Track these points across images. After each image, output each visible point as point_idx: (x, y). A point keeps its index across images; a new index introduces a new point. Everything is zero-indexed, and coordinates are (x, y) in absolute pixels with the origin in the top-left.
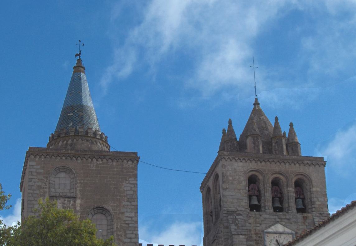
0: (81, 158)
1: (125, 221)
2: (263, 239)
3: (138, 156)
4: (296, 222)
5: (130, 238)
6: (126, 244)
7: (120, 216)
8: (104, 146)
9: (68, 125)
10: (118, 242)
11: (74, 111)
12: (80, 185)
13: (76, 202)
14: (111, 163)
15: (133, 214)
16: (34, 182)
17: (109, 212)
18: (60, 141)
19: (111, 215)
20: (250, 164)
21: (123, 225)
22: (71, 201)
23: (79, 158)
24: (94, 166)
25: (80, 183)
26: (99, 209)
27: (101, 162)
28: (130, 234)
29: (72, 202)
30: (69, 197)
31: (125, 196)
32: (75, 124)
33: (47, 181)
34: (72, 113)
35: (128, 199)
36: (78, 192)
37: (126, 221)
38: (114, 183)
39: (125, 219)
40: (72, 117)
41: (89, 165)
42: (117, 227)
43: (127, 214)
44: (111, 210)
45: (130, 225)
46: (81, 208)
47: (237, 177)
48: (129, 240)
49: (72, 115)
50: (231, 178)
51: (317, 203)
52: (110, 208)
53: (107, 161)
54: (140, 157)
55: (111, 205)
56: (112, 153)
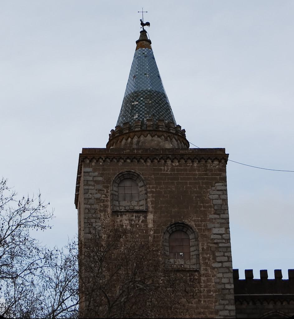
0: (150, 159)
1: (212, 239)
3: (226, 153)
6: (216, 270)
8: (181, 143)
9: (132, 118)
10: (205, 268)
11: (140, 99)
12: (151, 195)
13: (148, 217)
14: (191, 164)
15: (222, 231)
16: (91, 194)
17: (191, 228)
18: (122, 140)
19: (194, 232)
21: (211, 245)
22: (140, 216)
23: (149, 160)
24: (168, 169)
25: (152, 192)
26: (178, 226)
27: (178, 164)
28: (221, 256)
29: (142, 218)
30: (137, 212)
31: (211, 207)
32: (141, 116)
33: (107, 192)
34: (137, 101)
35: (216, 210)
36: (150, 205)
37: (215, 239)
38: (195, 190)
39: (212, 237)
40: (137, 106)
41: (163, 168)
42: (203, 249)
43: (215, 231)
44: (194, 226)
45: (220, 245)
46: (154, 225)
48: (220, 265)
49: (137, 104)
52: (192, 224)
53: (186, 162)
54: (228, 154)
55: (194, 219)
56: (191, 151)
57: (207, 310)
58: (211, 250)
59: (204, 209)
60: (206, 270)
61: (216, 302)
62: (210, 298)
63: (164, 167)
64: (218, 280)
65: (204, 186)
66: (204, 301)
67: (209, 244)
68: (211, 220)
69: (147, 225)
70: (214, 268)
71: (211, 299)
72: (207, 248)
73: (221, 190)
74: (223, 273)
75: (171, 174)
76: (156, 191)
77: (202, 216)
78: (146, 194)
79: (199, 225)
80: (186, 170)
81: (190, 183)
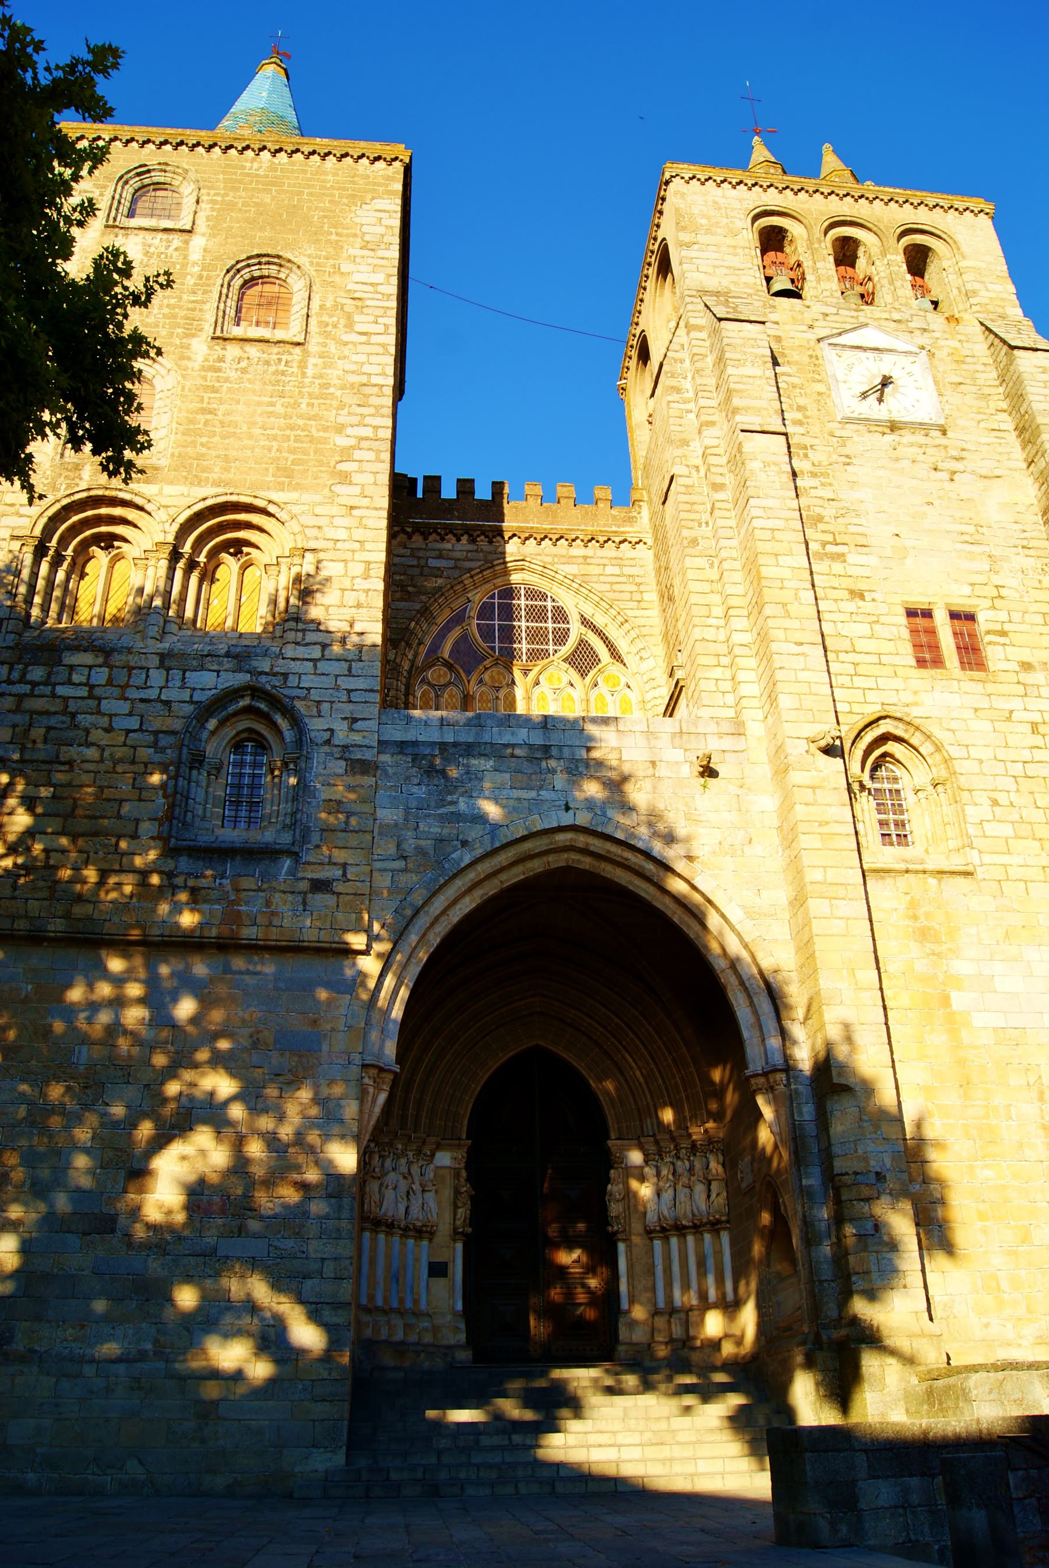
2: (821, 361)
4: (925, 330)
6: (350, 346)
7: (337, 279)
10: (321, 341)
20: (763, 194)
21: (344, 301)
23: (217, 149)
31: (355, 235)
41: (248, 165)
42: (322, 307)
44: (307, 264)
45: (369, 302)
47: (725, 220)
48: (364, 339)
50: (703, 221)
51: (983, 293)
55: (309, 252)
58: (342, 308)
59: (337, 238)
61: (342, 406)
63: (252, 162)
64: (354, 367)
65: (345, 200)
66: (308, 404)
68: (353, 259)
69: (185, 257)
70: (346, 344)
71: (328, 402)
72: (336, 306)
74: (369, 354)
75: (267, 176)
76: (223, 201)
77: (331, 250)
78: (198, 202)
79: (318, 264)
80: (305, 172)
81: (311, 194)
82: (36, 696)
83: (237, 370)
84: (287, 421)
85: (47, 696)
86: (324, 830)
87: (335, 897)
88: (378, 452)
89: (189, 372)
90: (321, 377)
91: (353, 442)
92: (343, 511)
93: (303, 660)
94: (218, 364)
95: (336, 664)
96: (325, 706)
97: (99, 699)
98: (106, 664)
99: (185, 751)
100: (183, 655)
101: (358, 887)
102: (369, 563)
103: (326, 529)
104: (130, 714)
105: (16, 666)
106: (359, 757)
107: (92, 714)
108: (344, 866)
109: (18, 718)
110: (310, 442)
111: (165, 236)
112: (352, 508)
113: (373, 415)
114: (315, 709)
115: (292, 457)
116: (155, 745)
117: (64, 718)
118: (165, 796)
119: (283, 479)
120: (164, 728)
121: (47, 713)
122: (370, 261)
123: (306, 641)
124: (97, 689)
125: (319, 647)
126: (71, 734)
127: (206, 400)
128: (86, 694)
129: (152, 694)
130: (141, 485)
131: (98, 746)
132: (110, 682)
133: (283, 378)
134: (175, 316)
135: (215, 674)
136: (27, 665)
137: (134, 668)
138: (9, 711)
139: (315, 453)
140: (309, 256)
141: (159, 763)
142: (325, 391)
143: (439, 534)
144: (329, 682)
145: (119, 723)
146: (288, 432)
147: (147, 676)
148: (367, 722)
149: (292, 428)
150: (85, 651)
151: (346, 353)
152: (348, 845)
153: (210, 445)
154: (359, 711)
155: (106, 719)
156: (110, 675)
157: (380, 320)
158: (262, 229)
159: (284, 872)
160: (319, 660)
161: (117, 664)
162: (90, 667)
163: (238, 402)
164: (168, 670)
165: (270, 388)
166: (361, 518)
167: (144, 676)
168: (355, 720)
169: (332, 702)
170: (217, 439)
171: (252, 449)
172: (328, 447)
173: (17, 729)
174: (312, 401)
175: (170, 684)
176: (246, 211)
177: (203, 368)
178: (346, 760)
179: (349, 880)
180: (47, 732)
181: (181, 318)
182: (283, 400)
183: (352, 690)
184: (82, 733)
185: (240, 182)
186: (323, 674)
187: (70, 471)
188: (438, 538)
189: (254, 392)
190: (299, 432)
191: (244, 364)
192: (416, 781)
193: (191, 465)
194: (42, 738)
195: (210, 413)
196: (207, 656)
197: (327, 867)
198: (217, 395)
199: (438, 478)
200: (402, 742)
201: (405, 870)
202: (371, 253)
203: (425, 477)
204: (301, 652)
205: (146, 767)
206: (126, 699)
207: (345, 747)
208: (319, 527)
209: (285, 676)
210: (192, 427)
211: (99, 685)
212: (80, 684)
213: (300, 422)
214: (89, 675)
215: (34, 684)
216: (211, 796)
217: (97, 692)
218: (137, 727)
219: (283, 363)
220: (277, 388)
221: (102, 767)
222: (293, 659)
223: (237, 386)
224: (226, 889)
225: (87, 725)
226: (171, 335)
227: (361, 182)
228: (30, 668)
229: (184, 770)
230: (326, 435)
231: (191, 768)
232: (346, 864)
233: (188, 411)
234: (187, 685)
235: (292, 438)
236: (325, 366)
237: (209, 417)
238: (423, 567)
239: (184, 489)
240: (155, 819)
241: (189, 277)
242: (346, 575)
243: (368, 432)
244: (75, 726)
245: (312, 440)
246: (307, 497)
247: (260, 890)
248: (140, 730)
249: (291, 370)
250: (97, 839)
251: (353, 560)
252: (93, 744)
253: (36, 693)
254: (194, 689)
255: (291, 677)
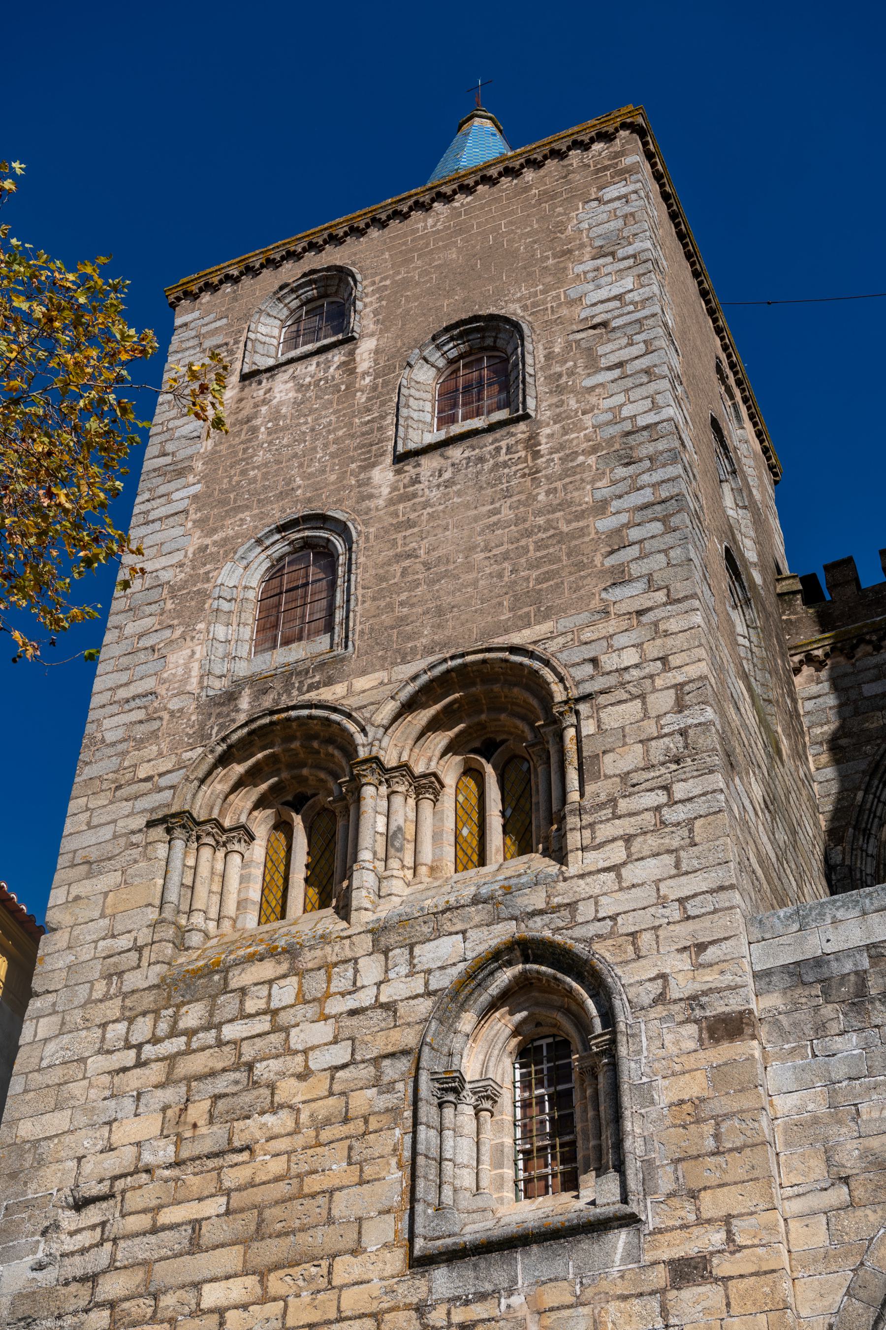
5: (620, 365)
7: (565, 311)
10: (555, 400)
13: (358, 351)
21: (579, 336)
31: (582, 246)
37: (593, 317)
42: (549, 357)
44: (519, 311)
45: (614, 324)
48: (617, 373)
55: (519, 295)
57: (559, 514)
60: (561, 403)
62: (575, 474)
64: (609, 416)
66: (548, 493)
67: (571, 337)
69: (352, 372)
70: (592, 389)
71: (578, 477)
72: (568, 346)
73: (619, 198)
75: (447, 228)
76: (394, 282)
79: (534, 305)
81: (511, 223)
82: (194, 1051)
83: (438, 486)
84: (521, 527)
85: (210, 1047)
86: (679, 1160)
87: (720, 1289)
88: (664, 520)
89: (373, 513)
90: (562, 447)
91: (624, 518)
92: (625, 624)
93: (599, 871)
94: (412, 489)
95: (652, 862)
96: (646, 939)
97: (286, 1030)
98: (294, 971)
99: (424, 1077)
100: (404, 921)
101: (760, 1259)
102: (682, 685)
103: (603, 658)
104: (335, 1041)
105: (164, 1013)
106: (720, 1010)
107: (277, 1057)
108: (728, 1219)
109: (172, 1095)
110: (559, 542)
111: (322, 358)
112: (640, 613)
113: (650, 470)
114: (630, 948)
115: (534, 574)
116: (376, 1083)
117: (237, 1075)
118: (400, 1166)
119: (526, 609)
120: (390, 1049)
121: (213, 1074)
122: (609, 269)
123: (598, 841)
124: (282, 1014)
125: (621, 843)
126: (247, 1098)
127: (400, 542)
128: (267, 1027)
129: (365, 998)
130: (321, 690)
131: (290, 1107)
132: (302, 999)
133: (506, 471)
134: (344, 451)
135: (460, 936)
136: (178, 1006)
137: (336, 965)
138: (156, 1087)
139: (569, 555)
140: (519, 300)
141: (387, 1110)
142: (571, 464)
143: (870, 642)
144: (645, 895)
145: (320, 1061)
146: (523, 542)
147: (356, 971)
148: (724, 945)
149: (528, 533)
150: (261, 960)
151: (593, 400)
152: (728, 1178)
153: (415, 600)
154: (703, 930)
155: (300, 1058)
156: (300, 985)
157: (637, 338)
158: (449, 294)
159: (618, 1257)
160: (624, 864)
161: (310, 965)
162: (270, 982)
163: (446, 529)
164: (386, 952)
165: (489, 491)
166: (656, 624)
167: (350, 973)
168: (701, 947)
169: (656, 928)
170: (419, 591)
171: (475, 583)
172: (587, 539)
173: (169, 1113)
174: (552, 486)
175: (392, 975)
176: (427, 282)
177: (391, 502)
178: (696, 1021)
179: (741, 1248)
180: (214, 1104)
181: (355, 449)
182: (509, 501)
183: (688, 898)
184: (266, 1092)
185: (411, 250)
186: (633, 886)
187: (223, 704)
188: (869, 648)
189: (467, 506)
190: (541, 535)
191: (447, 475)
192: (834, 1027)
193: (390, 636)
194: (207, 1116)
195: (409, 556)
196: (443, 912)
197: (696, 1231)
198: (416, 530)
199: (849, 561)
200: (797, 963)
201: (852, 1205)
202: (609, 259)
203: (827, 568)
204: (594, 859)
205: (366, 1122)
206: (326, 1018)
207: (694, 998)
208: (594, 661)
209: (572, 906)
210: (384, 585)
211: (284, 1008)
212: (258, 1014)
213: (541, 521)
214: (270, 995)
215: (190, 1033)
216: (485, 1149)
217: (284, 1018)
218: (347, 1058)
219: (504, 451)
220: (501, 487)
221: (299, 1141)
222: (582, 876)
223: (441, 507)
224: (519, 1314)
225: (272, 1076)
226: (342, 477)
227: (578, 177)
228: (183, 1010)
229: (428, 1112)
230: (581, 524)
231: (440, 1106)
232: (730, 1216)
233: (376, 566)
234: (418, 968)
235: (531, 548)
236: (565, 431)
237: (407, 563)
238: (855, 701)
239: (382, 675)
240: (388, 1212)
241: (359, 394)
242: (646, 716)
243: (647, 496)
244: (255, 1083)
245: (561, 537)
246: (565, 623)
247: (580, 1303)
248: (352, 1062)
249: (516, 456)
250: (297, 1271)
251: (655, 690)
252: (281, 1106)
253: (194, 1046)
254: (429, 972)
255: (581, 906)
